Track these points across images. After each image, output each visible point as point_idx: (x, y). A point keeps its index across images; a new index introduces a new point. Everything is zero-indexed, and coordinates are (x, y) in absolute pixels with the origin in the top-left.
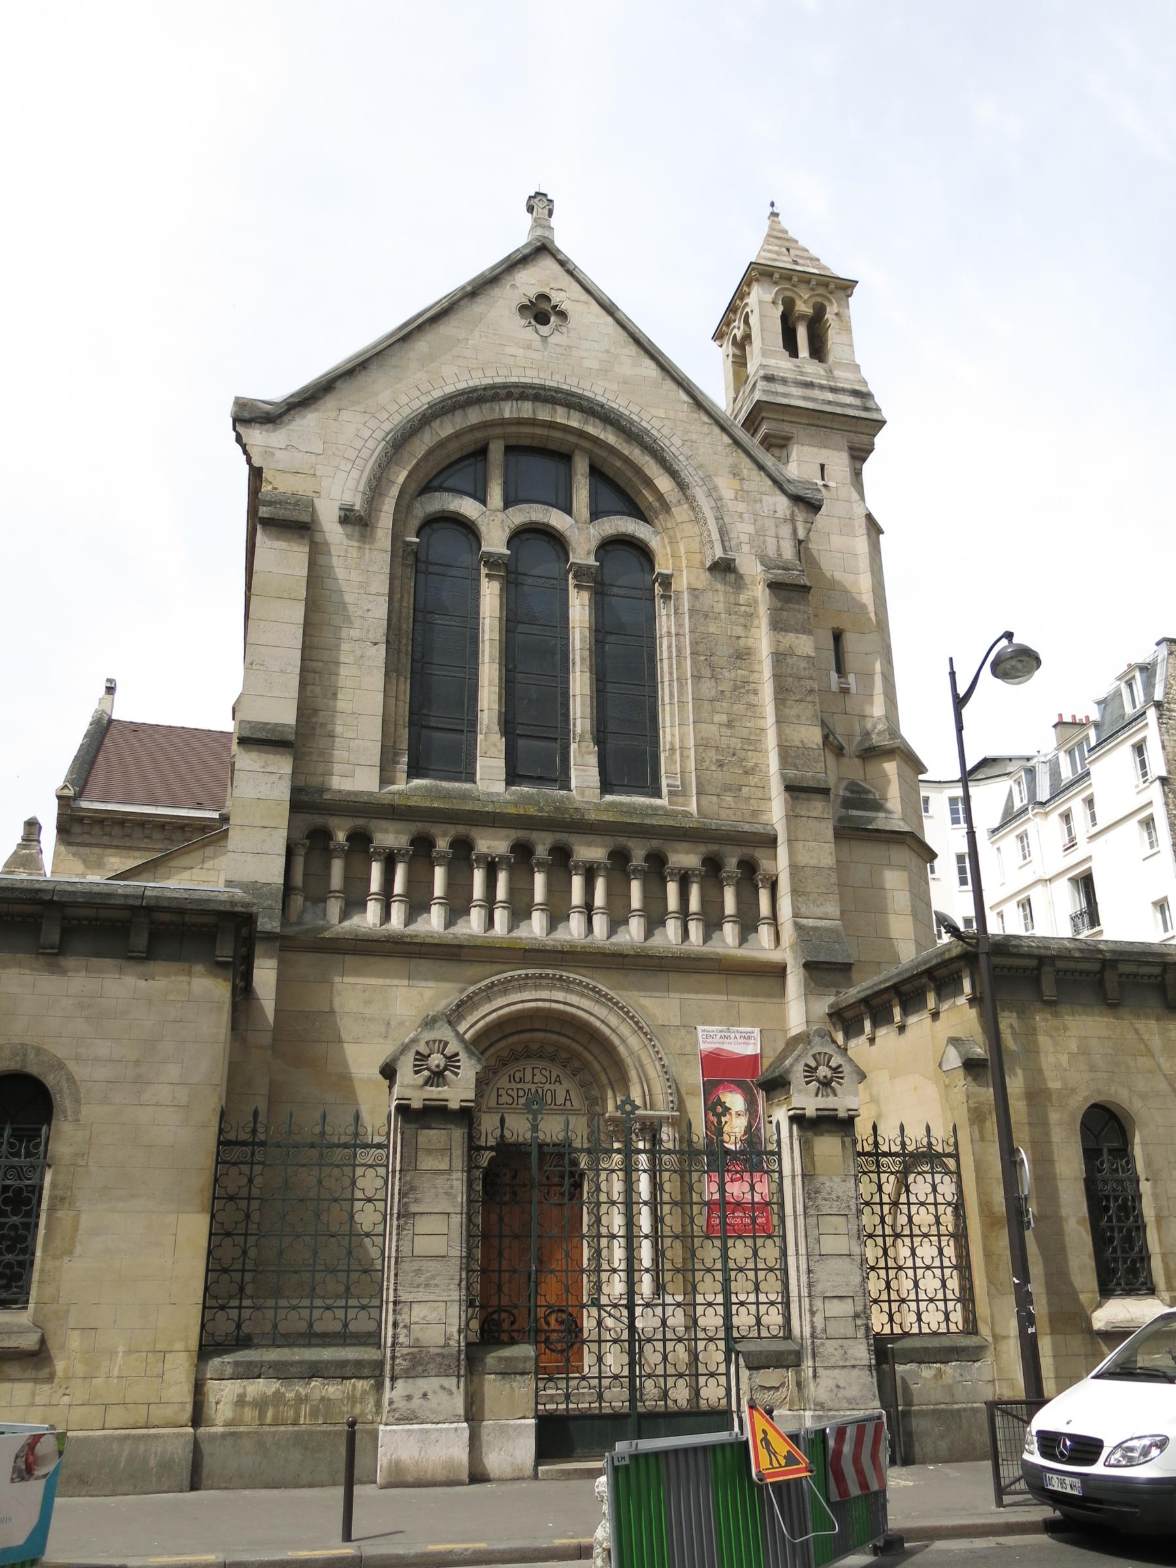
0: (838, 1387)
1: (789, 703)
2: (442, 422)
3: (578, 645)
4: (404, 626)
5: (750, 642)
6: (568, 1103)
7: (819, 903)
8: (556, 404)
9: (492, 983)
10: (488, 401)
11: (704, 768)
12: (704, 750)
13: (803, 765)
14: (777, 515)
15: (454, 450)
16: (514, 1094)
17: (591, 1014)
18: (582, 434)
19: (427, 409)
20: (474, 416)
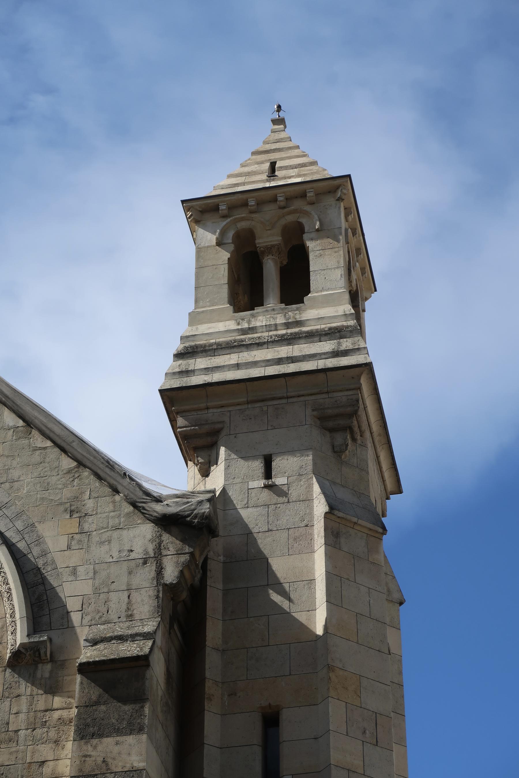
14: (133, 555)
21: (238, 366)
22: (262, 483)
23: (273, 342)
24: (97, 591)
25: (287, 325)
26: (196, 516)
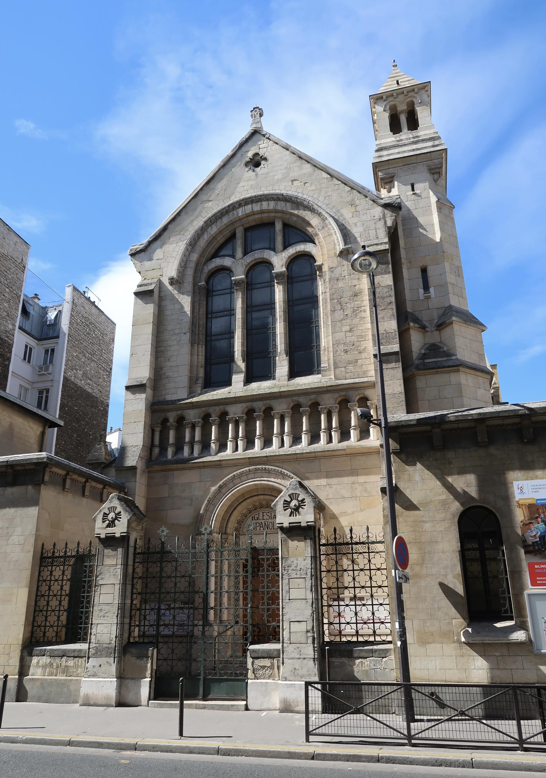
0: (295, 669)
2: (212, 228)
4: (201, 323)
5: (361, 286)
7: (393, 412)
8: (262, 201)
9: (234, 475)
10: (231, 211)
11: (337, 355)
12: (337, 346)
13: (386, 342)
14: (375, 218)
15: (221, 239)
17: (280, 484)
18: (276, 211)
20: (225, 220)
21: (399, 153)
22: (412, 193)
23: (410, 144)
24: (365, 230)
25: (414, 138)
26: (396, 203)
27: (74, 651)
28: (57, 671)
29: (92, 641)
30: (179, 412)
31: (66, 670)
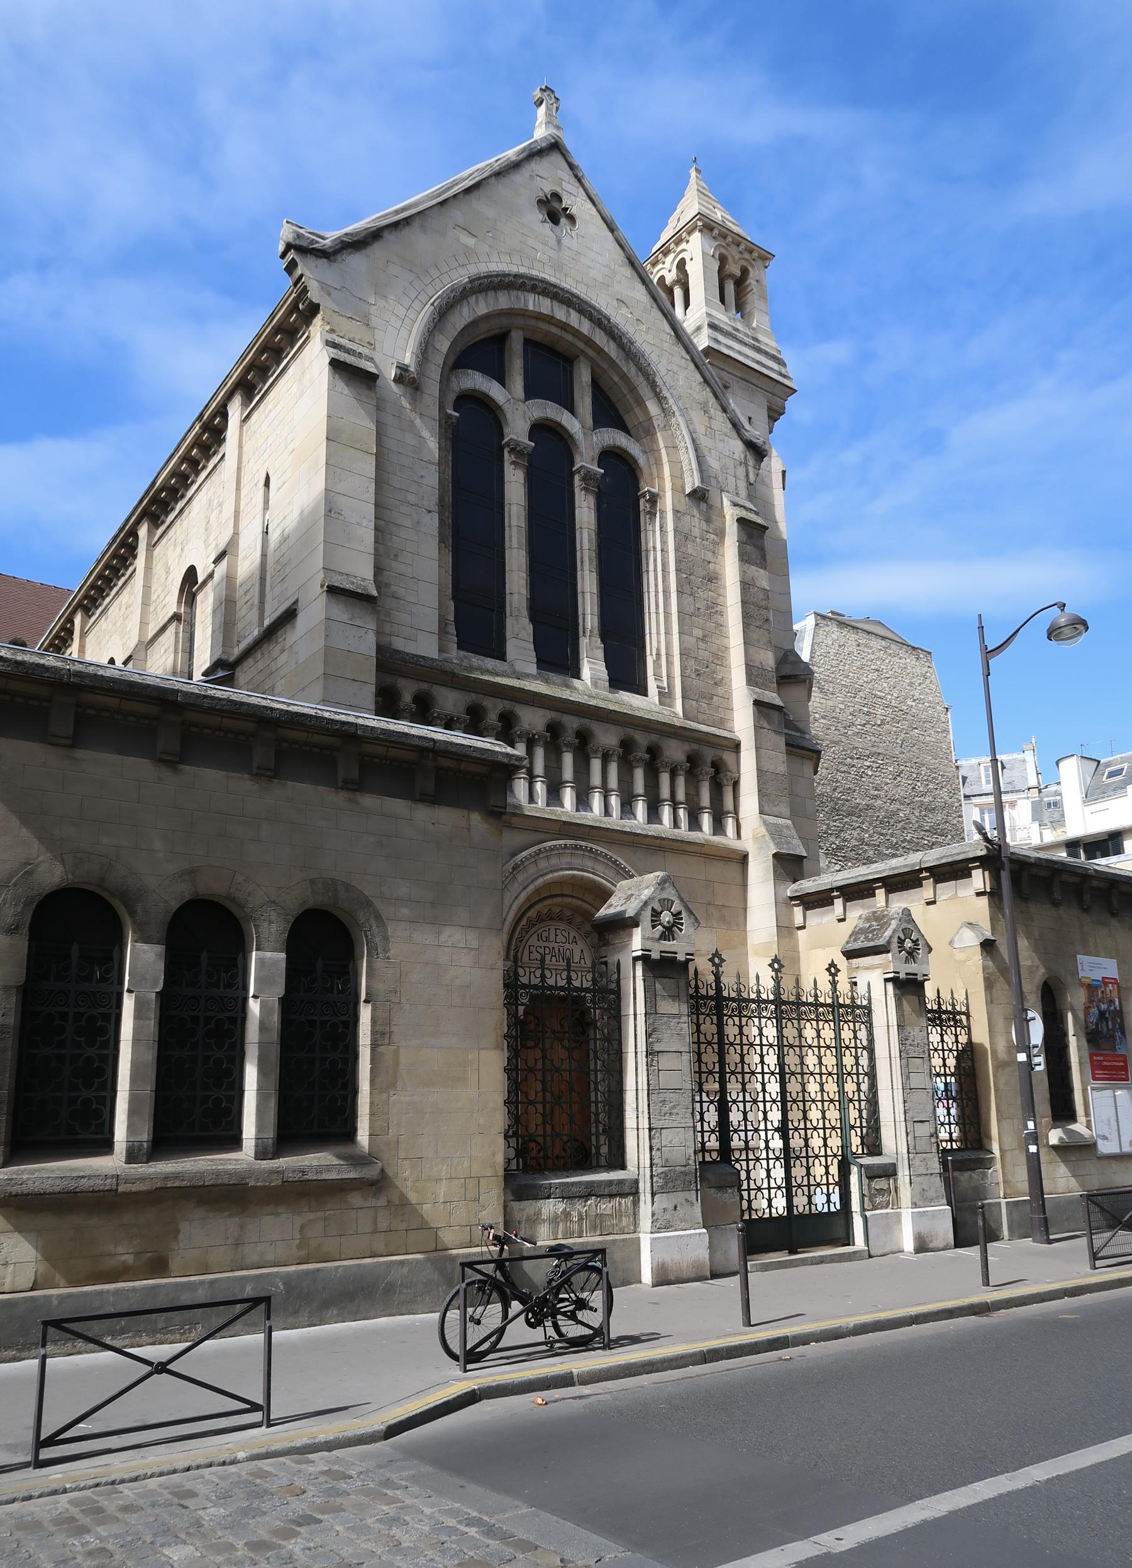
1: (752, 627)
3: (586, 546)
6: (582, 960)
16: (542, 951)
18: (589, 341)
19: (466, 283)
20: (504, 301)
21: (740, 353)
27: (610, 1183)
28: (580, 1226)
29: (655, 1161)
30: (424, 686)
31: (598, 1223)
